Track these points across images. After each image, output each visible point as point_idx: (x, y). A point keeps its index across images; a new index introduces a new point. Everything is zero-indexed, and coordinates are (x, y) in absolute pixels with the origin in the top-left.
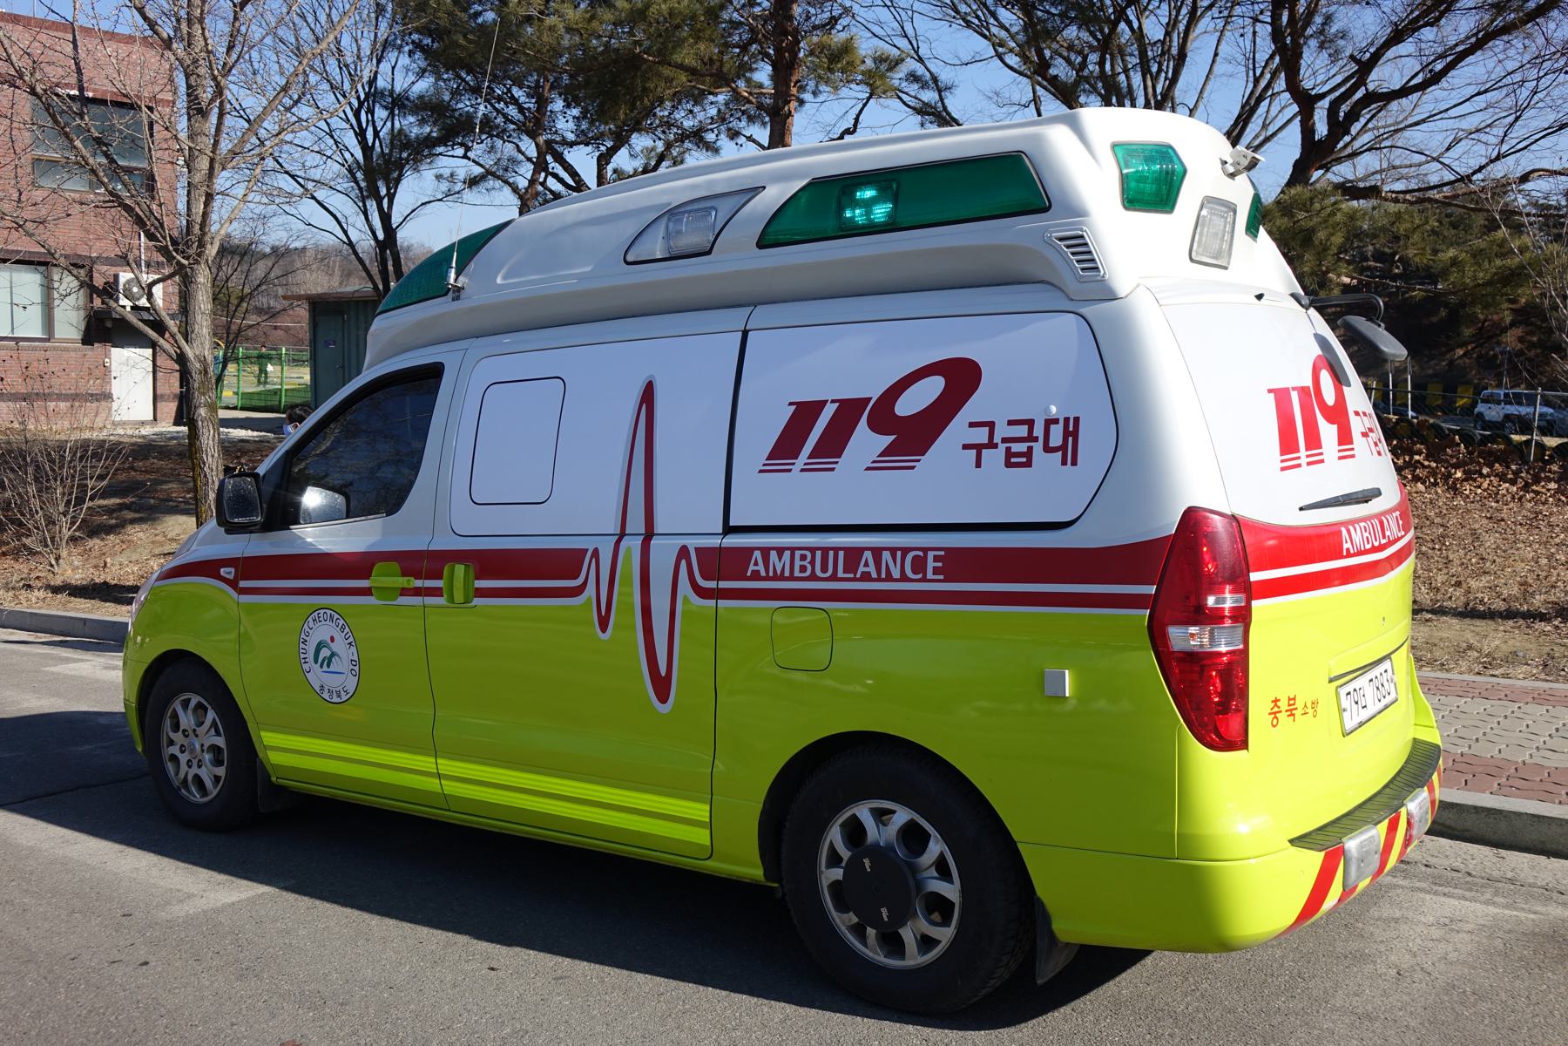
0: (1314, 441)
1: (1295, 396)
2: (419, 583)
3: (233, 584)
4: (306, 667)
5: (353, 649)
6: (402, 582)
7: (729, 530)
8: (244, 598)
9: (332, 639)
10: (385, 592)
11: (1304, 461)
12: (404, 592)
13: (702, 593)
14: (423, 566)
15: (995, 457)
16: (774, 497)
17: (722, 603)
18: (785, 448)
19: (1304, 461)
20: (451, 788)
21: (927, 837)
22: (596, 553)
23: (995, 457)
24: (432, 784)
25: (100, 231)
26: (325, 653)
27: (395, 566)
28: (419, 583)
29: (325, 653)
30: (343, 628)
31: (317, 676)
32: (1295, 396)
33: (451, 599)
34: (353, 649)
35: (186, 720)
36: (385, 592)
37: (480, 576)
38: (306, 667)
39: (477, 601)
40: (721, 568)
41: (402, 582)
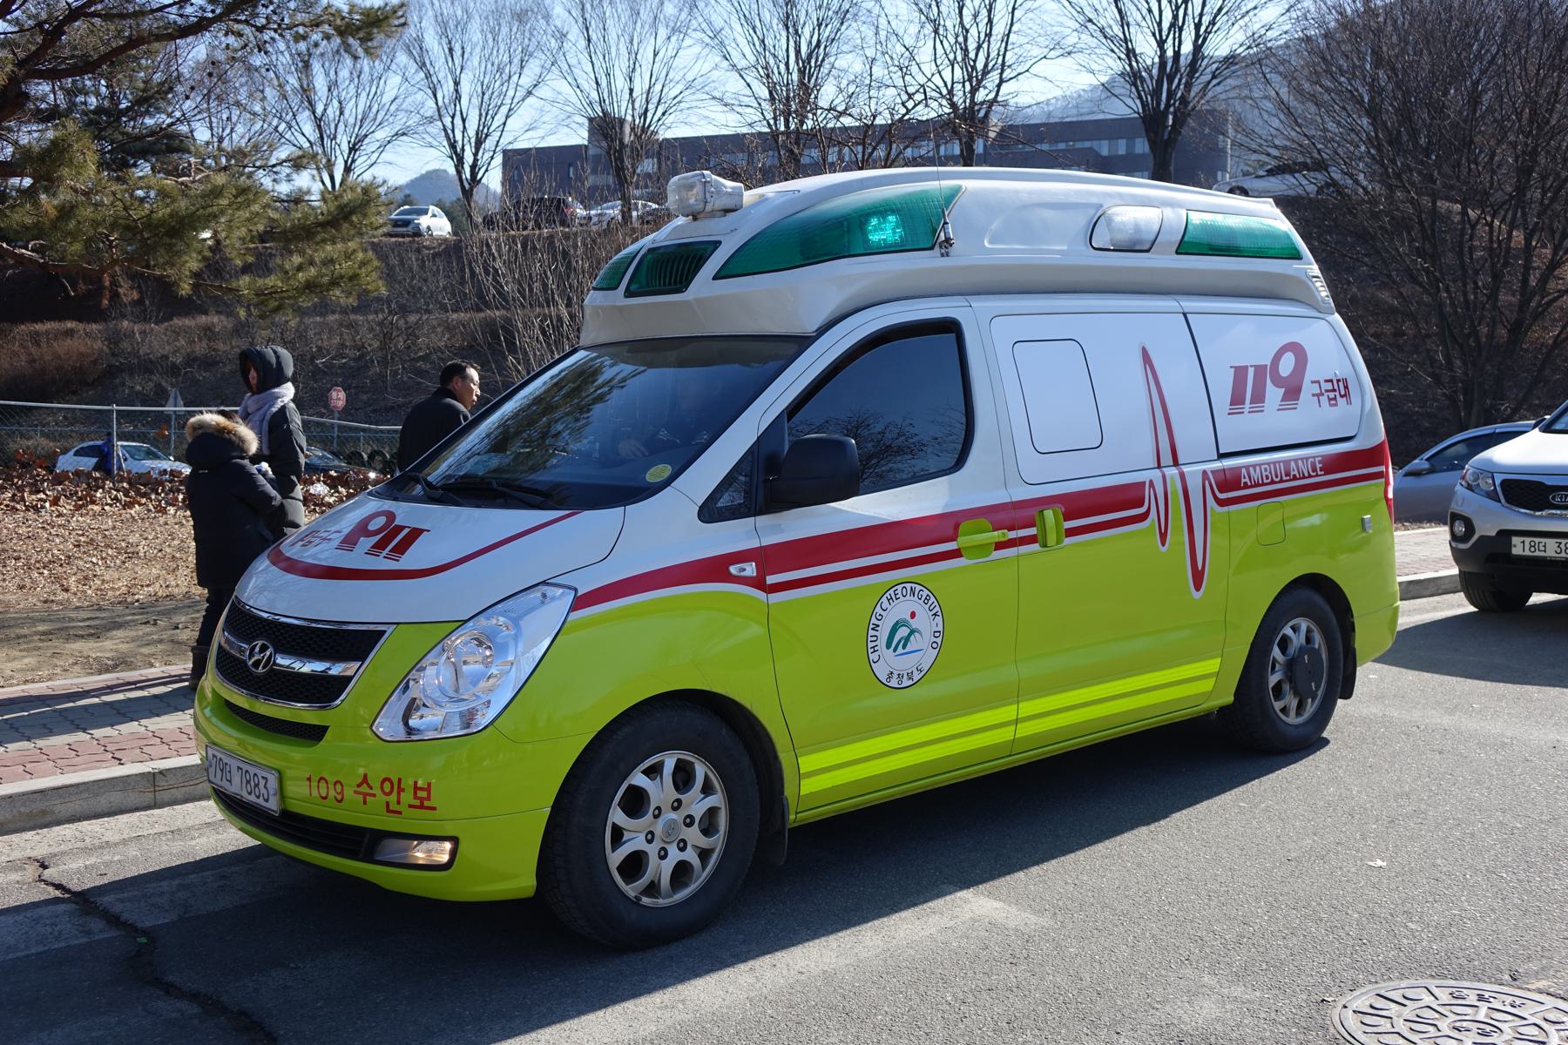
0: (1259, 397)
1: (1251, 372)
2: (1012, 535)
3: (758, 583)
4: (874, 657)
5: (939, 619)
6: (998, 536)
7: (1222, 456)
8: (776, 597)
9: (913, 615)
10: (981, 549)
11: (1246, 410)
12: (1000, 546)
13: (1221, 503)
14: (1015, 521)
15: (1324, 399)
16: (1243, 429)
17: (1233, 508)
18: (1237, 400)
19: (1246, 410)
20: (1026, 730)
21: (619, 869)
22: (1151, 483)
23: (1324, 399)
24: (1005, 735)
25: (398, 79)
26: (903, 632)
27: (984, 522)
28: (1012, 535)
29: (903, 632)
30: (927, 599)
31: (888, 662)
32: (1251, 372)
33: (1045, 545)
34: (939, 619)
35: (660, 791)
36: (981, 549)
37: (1067, 517)
38: (874, 657)
39: (1068, 541)
40: (1228, 486)
41: (998, 536)
